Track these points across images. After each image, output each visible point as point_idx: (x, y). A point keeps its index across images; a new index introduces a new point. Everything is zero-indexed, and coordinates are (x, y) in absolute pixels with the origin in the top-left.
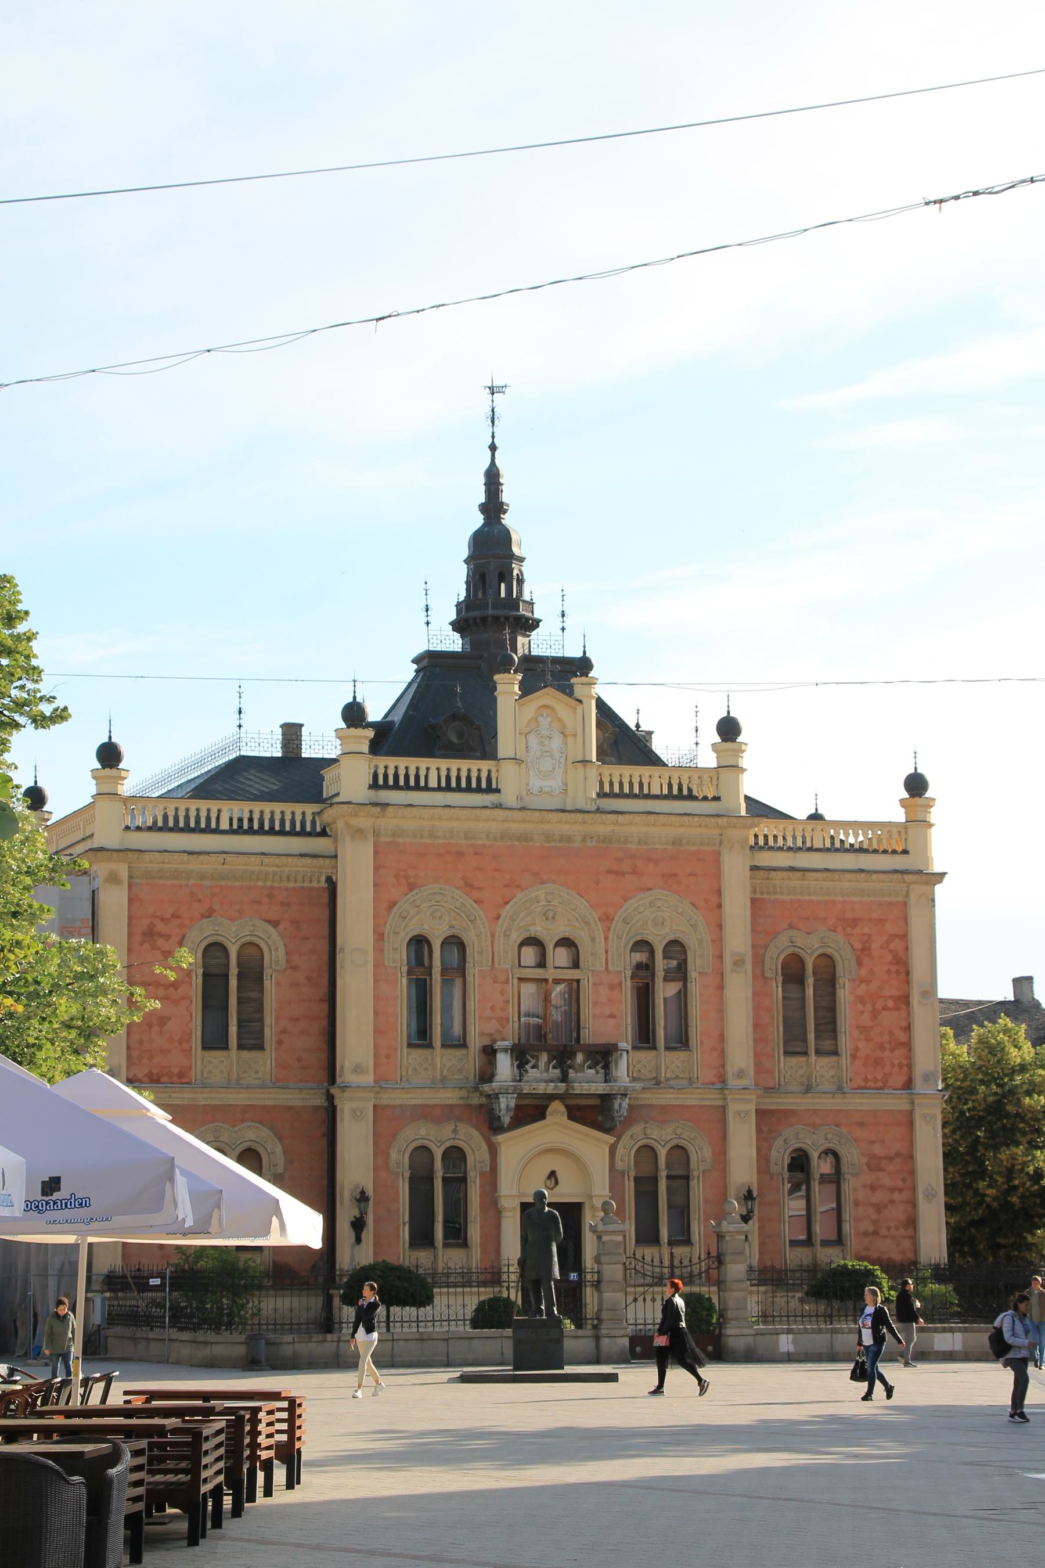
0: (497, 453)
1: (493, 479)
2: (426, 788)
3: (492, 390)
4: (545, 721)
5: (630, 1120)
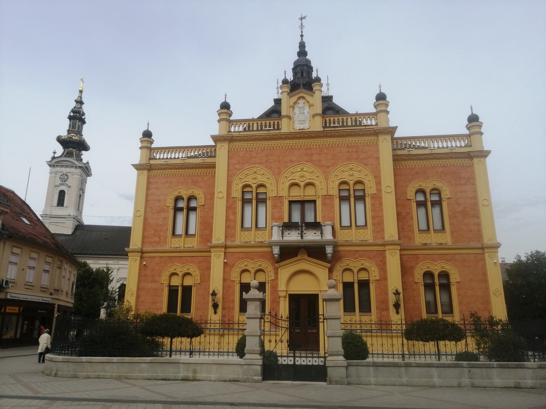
0: (303, 37)
1: (302, 45)
2: (253, 130)
3: (301, 19)
4: (301, 101)
5: (337, 257)
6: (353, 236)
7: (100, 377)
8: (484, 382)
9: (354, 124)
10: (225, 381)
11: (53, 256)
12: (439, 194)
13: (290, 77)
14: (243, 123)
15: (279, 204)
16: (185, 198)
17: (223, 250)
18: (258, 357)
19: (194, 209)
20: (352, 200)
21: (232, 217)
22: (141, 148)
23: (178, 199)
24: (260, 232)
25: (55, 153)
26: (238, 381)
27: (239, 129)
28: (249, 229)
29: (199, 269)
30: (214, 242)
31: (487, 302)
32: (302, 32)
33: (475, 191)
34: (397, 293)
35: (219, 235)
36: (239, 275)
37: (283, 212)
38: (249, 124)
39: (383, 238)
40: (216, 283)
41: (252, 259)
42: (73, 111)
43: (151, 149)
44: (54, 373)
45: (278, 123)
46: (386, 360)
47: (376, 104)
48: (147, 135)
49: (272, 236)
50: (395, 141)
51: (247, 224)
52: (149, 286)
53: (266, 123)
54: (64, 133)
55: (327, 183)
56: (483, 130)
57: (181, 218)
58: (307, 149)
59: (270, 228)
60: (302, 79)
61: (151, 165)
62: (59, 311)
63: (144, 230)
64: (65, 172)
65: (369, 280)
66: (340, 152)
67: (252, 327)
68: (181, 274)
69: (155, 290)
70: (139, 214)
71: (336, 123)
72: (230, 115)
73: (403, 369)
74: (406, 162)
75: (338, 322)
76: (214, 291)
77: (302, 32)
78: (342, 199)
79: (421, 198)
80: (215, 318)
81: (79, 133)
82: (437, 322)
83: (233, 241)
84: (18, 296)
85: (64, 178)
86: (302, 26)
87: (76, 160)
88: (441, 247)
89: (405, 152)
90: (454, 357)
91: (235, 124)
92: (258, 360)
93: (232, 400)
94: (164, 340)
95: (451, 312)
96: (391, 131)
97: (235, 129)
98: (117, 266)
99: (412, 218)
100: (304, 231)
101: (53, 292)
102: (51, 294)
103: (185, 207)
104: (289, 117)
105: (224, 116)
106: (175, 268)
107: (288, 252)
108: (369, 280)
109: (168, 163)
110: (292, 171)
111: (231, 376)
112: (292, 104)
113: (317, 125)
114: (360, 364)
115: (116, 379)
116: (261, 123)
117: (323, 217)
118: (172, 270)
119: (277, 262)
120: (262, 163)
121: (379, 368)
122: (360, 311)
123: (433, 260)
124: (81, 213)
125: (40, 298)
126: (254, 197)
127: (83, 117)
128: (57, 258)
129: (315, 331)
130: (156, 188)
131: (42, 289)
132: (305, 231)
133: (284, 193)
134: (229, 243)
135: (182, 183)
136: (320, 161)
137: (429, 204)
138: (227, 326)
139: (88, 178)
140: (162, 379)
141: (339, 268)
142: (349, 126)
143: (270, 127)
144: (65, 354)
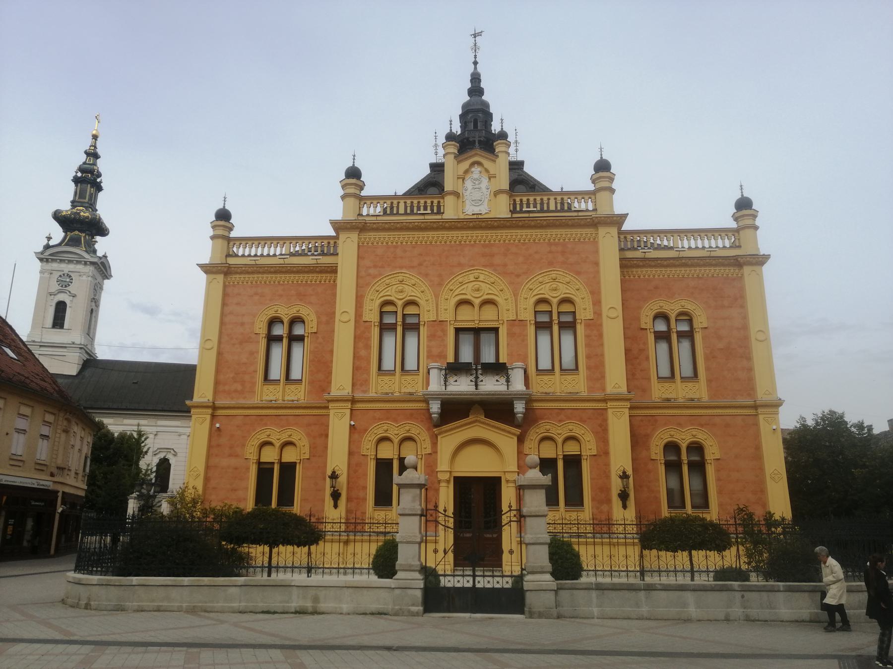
1: (476, 78)
2: (398, 214)
4: (476, 170)
5: (531, 418)
6: (557, 385)
7: (162, 609)
8: (765, 614)
9: (559, 208)
10: (365, 614)
11: (55, 412)
12: (690, 321)
13: (457, 129)
14: (382, 202)
15: (439, 333)
16: (286, 320)
17: (349, 405)
18: (417, 575)
19: (301, 339)
20: (556, 328)
21: (363, 353)
22: (212, 238)
23: (273, 321)
24: (409, 378)
25: (49, 238)
26: (385, 614)
27: (375, 211)
28: (392, 373)
29: (308, 435)
30: (335, 392)
31: (760, 489)
32: (475, 56)
33: (745, 317)
34: (624, 476)
35: (341, 382)
36: (374, 446)
37: (445, 346)
38: (392, 203)
39: (604, 390)
40: (337, 457)
41: (396, 421)
42: (81, 169)
43: (229, 240)
44: (83, 603)
45: (439, 202)
46: (616, 580)
47: (594, 177)
48: (223, 216)
49: (428, 384)
50: (622, 237)
51: (388, 364)
52: (225, 462)
53: (419, 202)
54: (65, 206)
55: (516, 301)
56: (758, 222)
57: (278, 353)
58: (484, 246)
59: (425, 371)
60: (476, 133)
61: (229, 266)
62: (64, 503)
63: (218, 371)
64: (66, 272)
65: (580, 455)
66: (536, 253)
67: (408, 529)
68: (278, 444)
69: (236, 469)
70: (209, 345)
71: (532, 206)
72: (362, 189)
73: (642, 594)
74: (639, 270)
75: (542, 520)
76: (334, 472)
77: (475, 56)
78: (540, 326)
79: (661, 327)
80: (333, 515)
81: (91, 205)
82: (688, 521)
83: (364, 392)
84: (12, 479)
85: (65, 282)
86: (475, 48)
87: (86, 251)
88: (692, 404)
89: (638, 254)
90: (712, 575)
91: (368, 202)
92: (418, 580)
93: (388, 643)
94: (251, 550)
95: (706, 505)
96: (618, 220)
97: (368, 211)
98: (154, 429)
99: (647, 358)
100: (480, 376)
101: (55, 471)
102: (52, 475)
103: (285, 335)
104: (457, 194)
105: (351, 190)
106: (268, 433)
107: (454, 410)
108: (580, 455)
109: (257, 262)
110: (461, 280)
111: (374, 607)
112: (461, 173)
113: (501, 209)
114: (566, 586)
115: (187, 612)
116: (412, 202)
117: (510, 355)
118: (263, 437)
119: (436, 426)
120: (413, 267)
121: (605, 592)
122: (567, 504)
123: (679, 425)
124: (93, 339)
125: (34, 481)
126: (399, 321)
127: (98, 180)
128: (62, 414)
129: (495, 536)
130: (238, 304)
131: (38, 467)
132: (481, 378)
133: (447, 315)
134: (359, 395)
135: (281, 296)
136: (505, 265)
137: (674, 337)
138: (354, 526)
139: (106, 281)
140: (263, 612)
141: (534, 435)
142: (552, 211)
143: (425, 209)
144: (97, 573)
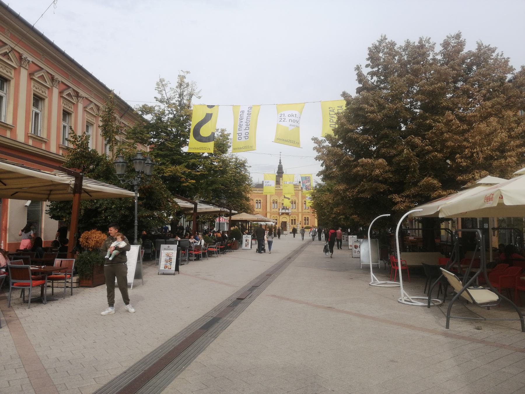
31: (314, 223)
